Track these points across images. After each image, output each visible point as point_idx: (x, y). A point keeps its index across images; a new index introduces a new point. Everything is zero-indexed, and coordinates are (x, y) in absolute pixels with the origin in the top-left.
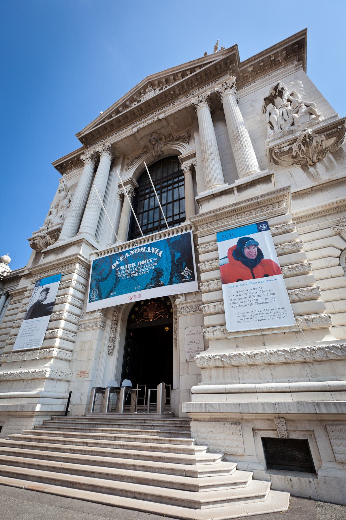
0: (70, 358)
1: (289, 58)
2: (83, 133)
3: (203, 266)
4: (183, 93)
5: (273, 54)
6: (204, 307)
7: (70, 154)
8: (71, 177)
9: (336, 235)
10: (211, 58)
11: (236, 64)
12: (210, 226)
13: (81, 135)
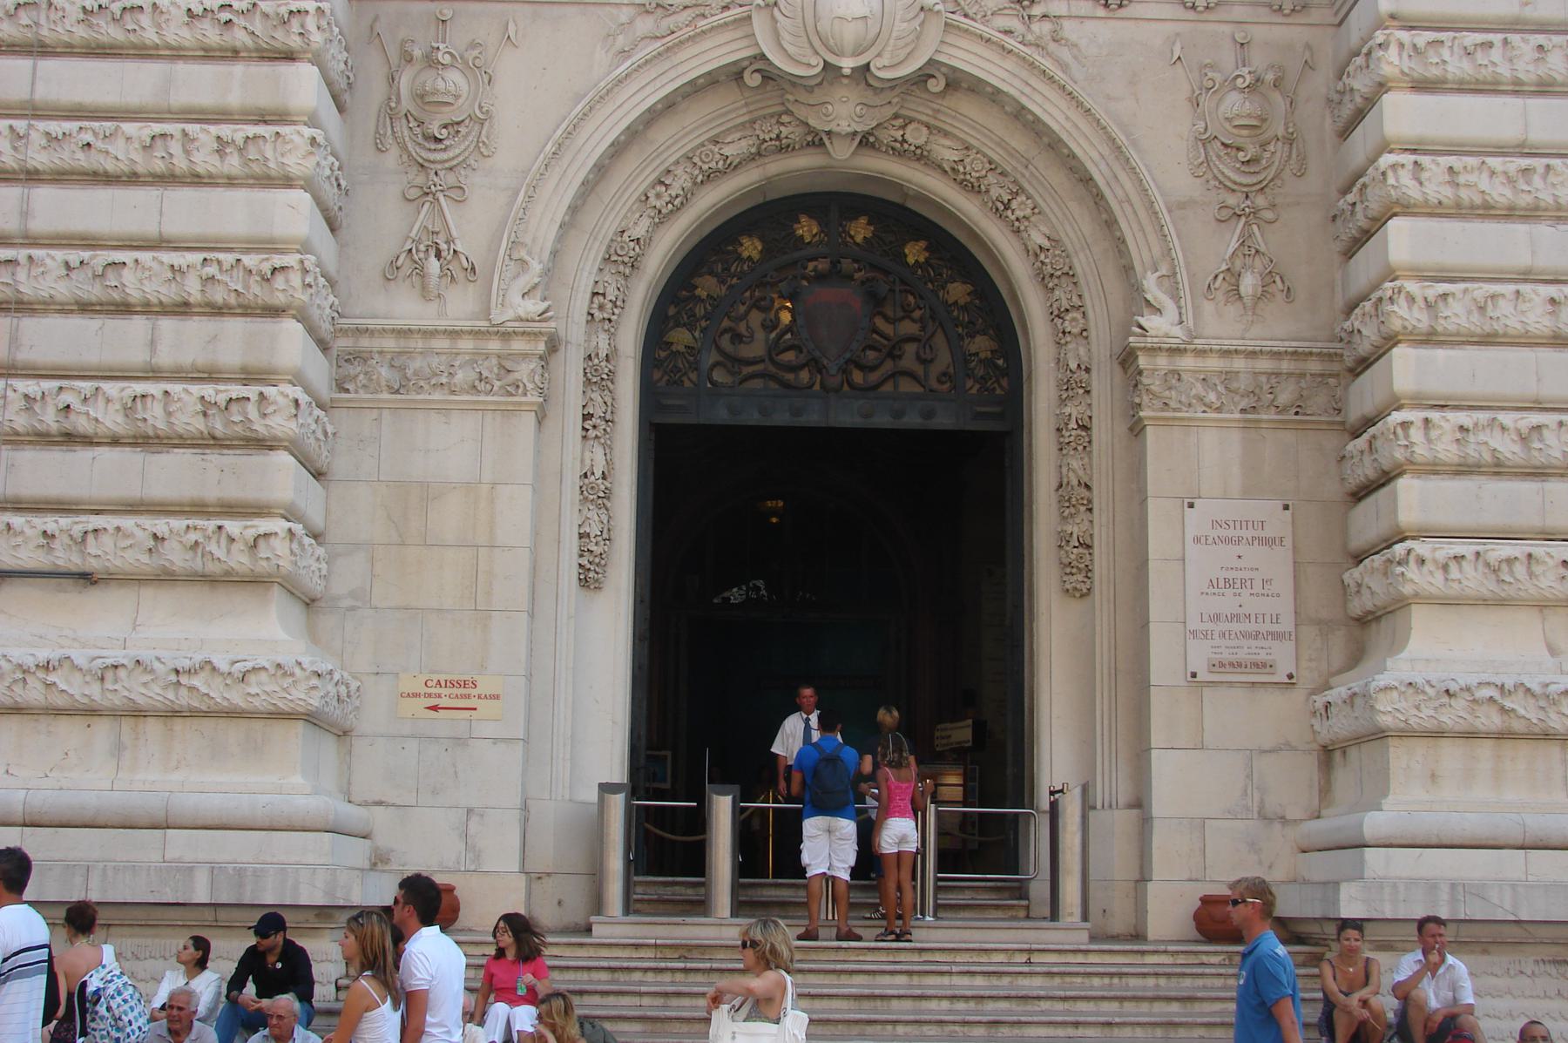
3: (1405, 178)
6: (1405, 425)
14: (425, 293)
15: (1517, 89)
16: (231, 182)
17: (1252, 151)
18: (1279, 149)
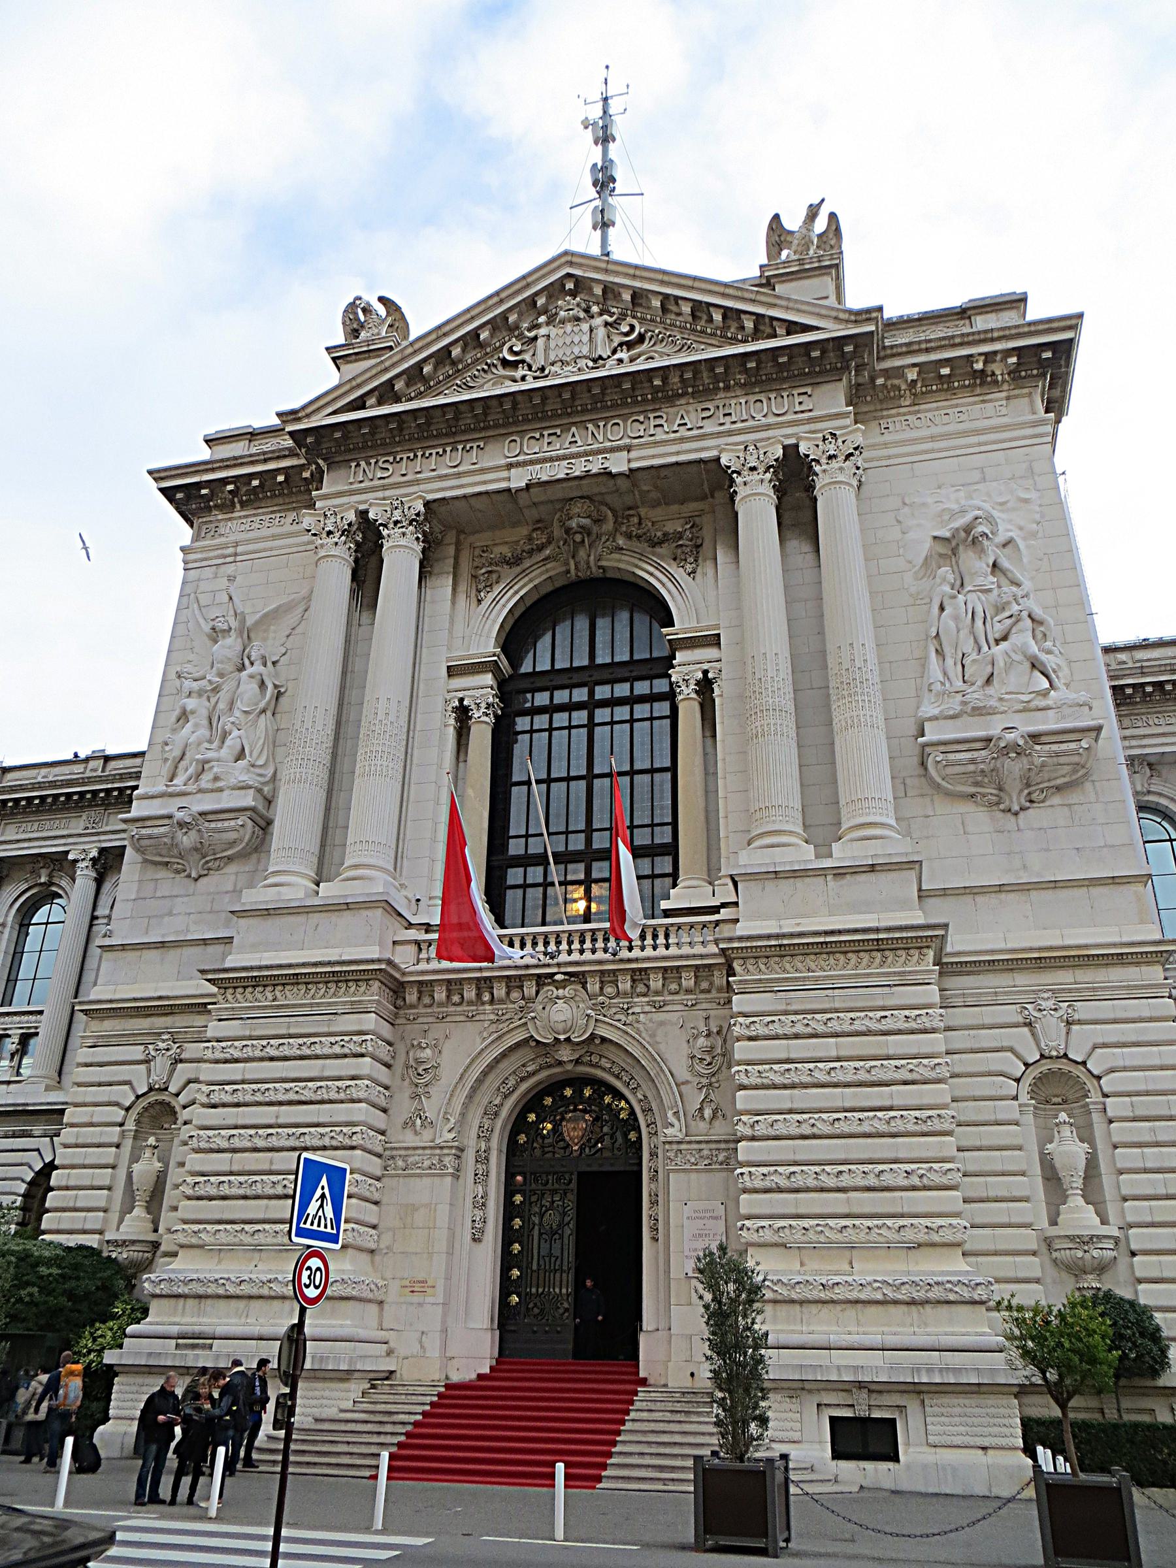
0: (373, 1246)
1: (1025, 377)
2: (308, 416)
4: (693, 393)
5: (980, 354)
7: (235, 458)
8: (236, 555)
9: (1025, 1025)
10: (799, 311)
11: (871, 353)
12: (763, 967)
13: (299, 420)
14: (416, 1133)
15: (786, 1037)
16: (342, 1102)
17: (709, 1060)
18: (720, 1058)
